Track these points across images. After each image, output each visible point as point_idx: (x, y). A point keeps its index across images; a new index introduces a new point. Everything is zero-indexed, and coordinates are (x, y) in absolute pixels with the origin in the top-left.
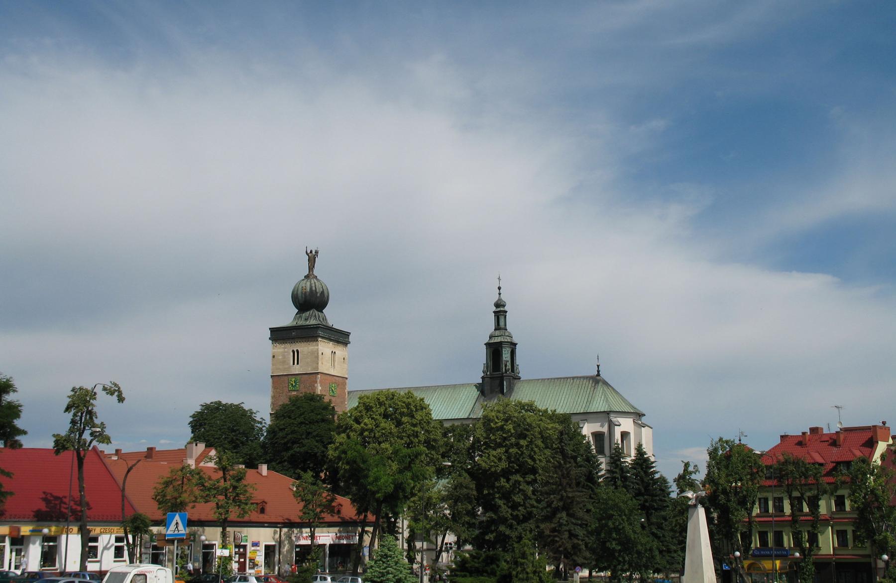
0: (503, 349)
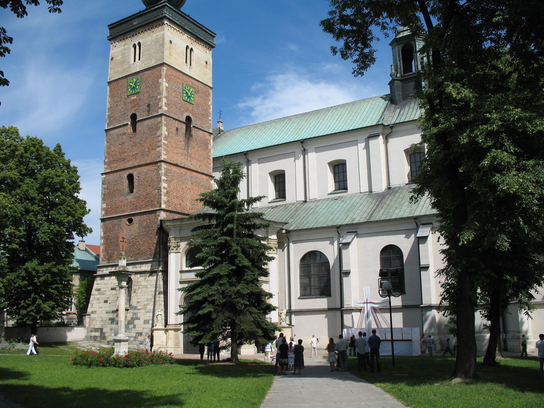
0: (417, 43)
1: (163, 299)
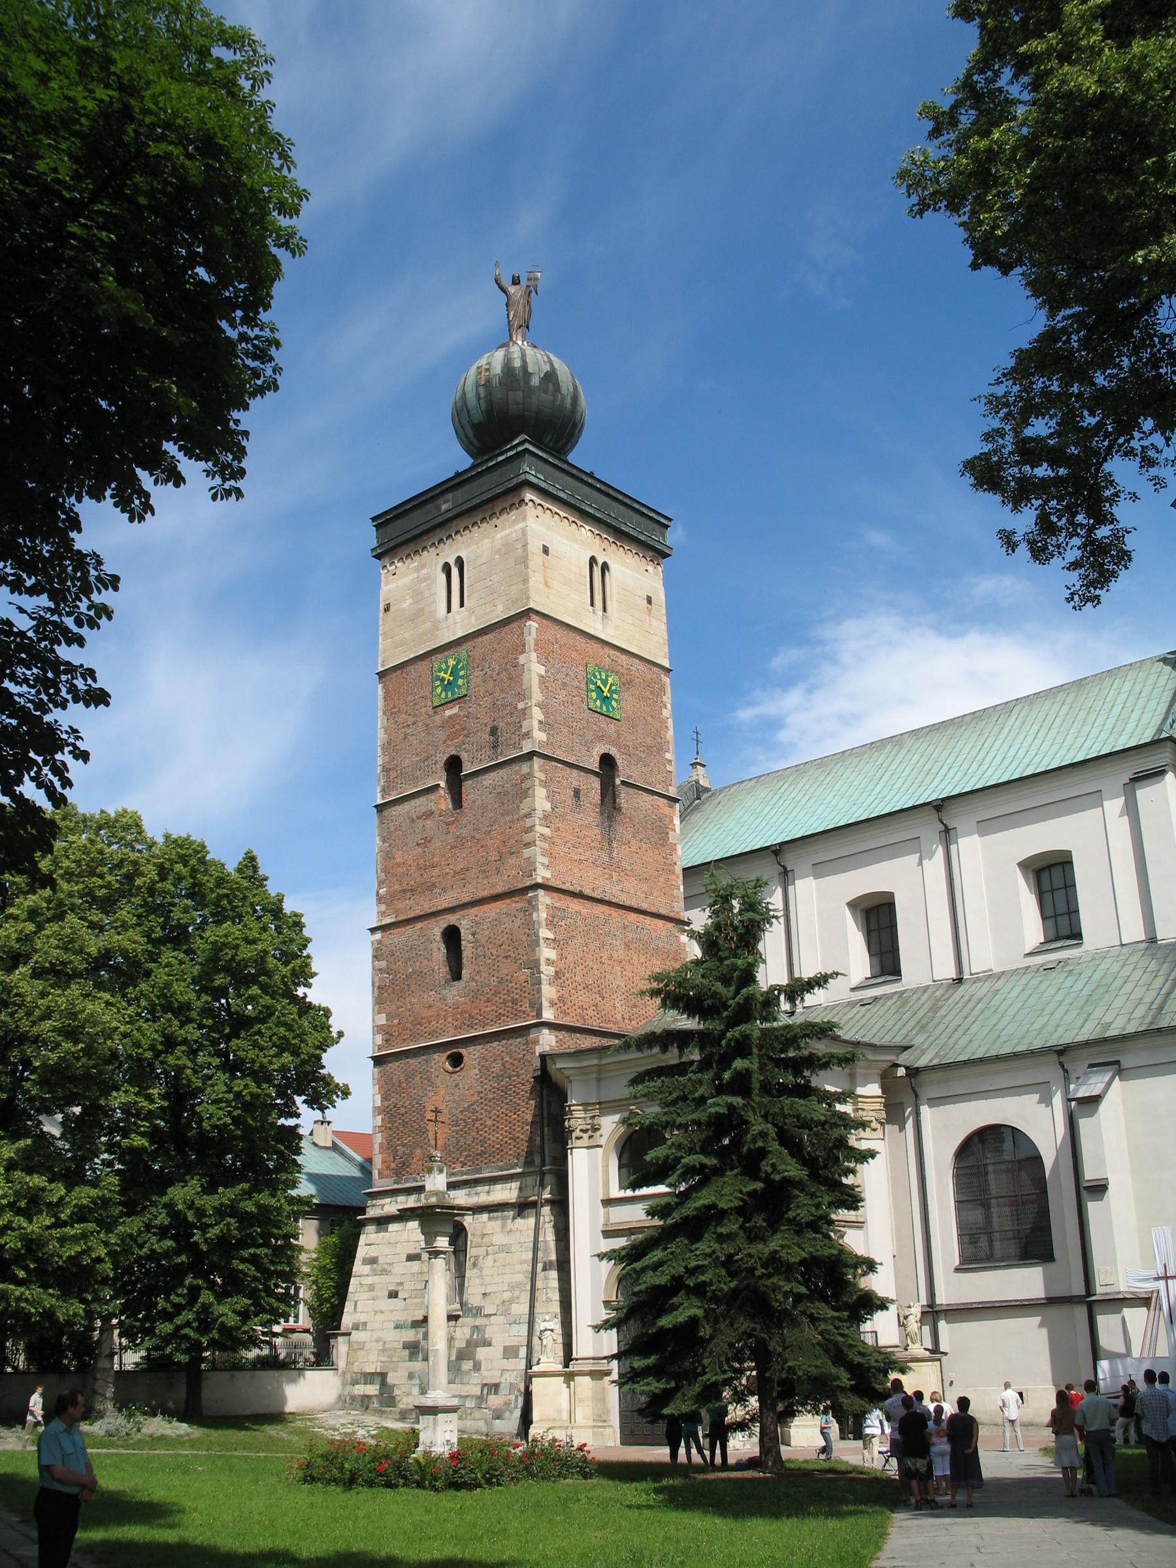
1: (555, 1284)
